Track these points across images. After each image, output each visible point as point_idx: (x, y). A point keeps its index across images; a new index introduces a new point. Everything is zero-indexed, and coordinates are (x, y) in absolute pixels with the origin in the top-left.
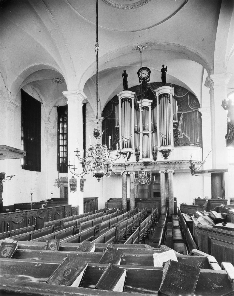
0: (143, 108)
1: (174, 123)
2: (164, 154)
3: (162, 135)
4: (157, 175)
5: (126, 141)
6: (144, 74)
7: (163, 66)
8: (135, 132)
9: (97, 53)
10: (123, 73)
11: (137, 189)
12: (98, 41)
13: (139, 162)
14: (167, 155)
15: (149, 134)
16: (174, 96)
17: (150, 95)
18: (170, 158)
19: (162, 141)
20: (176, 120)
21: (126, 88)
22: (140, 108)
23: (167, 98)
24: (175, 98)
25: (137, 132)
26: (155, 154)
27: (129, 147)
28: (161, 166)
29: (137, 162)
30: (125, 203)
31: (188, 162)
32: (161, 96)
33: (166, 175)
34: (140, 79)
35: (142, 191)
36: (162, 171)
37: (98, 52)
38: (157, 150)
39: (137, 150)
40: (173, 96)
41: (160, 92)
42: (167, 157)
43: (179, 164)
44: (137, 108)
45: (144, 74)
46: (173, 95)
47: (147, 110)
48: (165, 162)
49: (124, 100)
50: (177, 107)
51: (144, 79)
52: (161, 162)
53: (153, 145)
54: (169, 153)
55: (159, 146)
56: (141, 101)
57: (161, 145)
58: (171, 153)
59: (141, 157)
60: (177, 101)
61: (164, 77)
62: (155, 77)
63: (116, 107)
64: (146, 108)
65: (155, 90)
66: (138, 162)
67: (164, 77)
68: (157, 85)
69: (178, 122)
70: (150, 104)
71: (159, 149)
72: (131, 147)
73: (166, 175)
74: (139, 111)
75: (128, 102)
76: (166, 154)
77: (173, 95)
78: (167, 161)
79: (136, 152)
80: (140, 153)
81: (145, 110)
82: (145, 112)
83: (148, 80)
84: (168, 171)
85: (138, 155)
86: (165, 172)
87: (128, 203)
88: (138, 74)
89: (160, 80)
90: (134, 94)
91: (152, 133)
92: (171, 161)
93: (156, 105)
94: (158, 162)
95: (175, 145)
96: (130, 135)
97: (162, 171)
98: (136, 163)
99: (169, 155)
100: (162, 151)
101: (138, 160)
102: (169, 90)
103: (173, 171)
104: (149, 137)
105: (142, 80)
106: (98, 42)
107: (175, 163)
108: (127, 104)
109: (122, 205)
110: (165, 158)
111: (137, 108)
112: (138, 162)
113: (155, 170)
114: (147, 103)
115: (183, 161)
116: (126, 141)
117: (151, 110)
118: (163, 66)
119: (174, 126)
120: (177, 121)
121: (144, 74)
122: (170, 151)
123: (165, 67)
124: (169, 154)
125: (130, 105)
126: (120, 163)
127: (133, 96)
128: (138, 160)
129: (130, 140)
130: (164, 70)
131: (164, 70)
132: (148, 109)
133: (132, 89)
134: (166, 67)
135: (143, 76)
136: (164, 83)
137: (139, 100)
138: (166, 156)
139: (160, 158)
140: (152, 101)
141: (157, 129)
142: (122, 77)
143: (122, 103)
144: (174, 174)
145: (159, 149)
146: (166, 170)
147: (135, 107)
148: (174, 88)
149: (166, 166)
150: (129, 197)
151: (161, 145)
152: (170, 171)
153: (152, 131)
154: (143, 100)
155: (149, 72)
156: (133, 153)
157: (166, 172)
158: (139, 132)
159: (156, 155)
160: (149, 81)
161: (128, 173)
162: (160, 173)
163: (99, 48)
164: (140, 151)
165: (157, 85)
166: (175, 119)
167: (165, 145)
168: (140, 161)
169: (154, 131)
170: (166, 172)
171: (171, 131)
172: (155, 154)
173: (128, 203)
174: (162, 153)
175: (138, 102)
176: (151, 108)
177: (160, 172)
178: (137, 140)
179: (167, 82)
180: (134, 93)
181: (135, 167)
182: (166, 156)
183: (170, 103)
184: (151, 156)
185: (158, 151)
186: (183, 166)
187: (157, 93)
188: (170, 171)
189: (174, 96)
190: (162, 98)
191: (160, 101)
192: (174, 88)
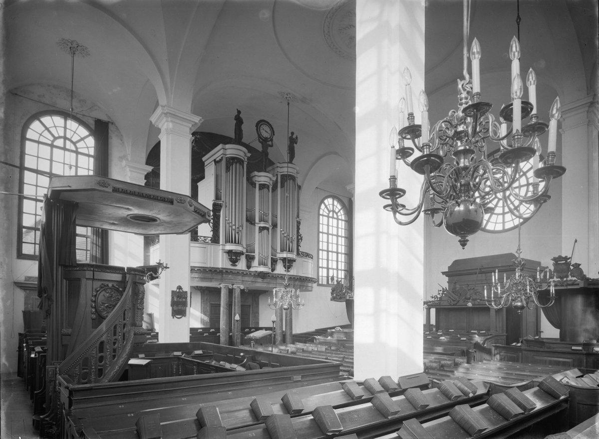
8: (247, 220)
18: (293, 272)
25: (251, 221)
26: (274, 262)
29: (247, 270)
39: (250, 249)
55: (279, 250)
59: (255, 263)
85: (250, 259)
88: (257, 126)
94: (279, 274)
100: (284, 260)
101: (249, 267)
128: (249, 267)
139: (280, 269)
164: (254, 253)
168: (251, 270)
169: (275, 226)
172: (274, 262)
178: (251, 234)
180: (249, 155)
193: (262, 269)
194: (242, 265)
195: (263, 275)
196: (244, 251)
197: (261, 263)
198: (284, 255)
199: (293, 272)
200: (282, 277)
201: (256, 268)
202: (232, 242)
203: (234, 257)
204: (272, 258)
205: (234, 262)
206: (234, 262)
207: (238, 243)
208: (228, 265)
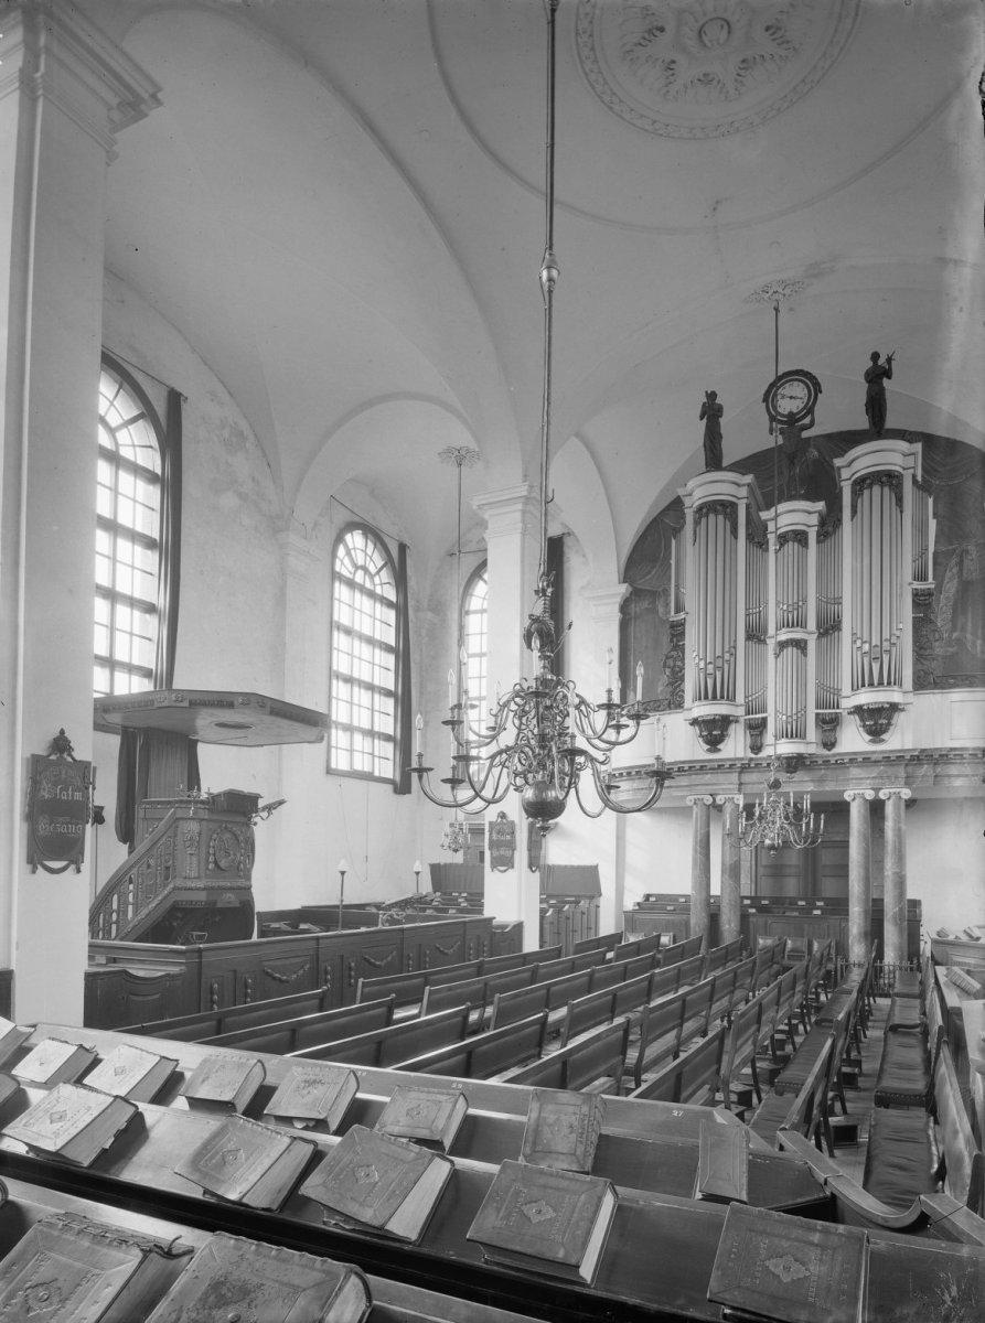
0: (783, 539)
1: (916, 594)
2: (715, 733)
3: (863, 643)
4: (837, 810)
5: (712, 671)
6: (791, 397)
7: (875, 356)
8: (750, 637)
9: (547, 295)
10: (704, 404)
11: (753, 862)
12: (554, 247)
13: (760, 755)
14: (882, 725)
15: (806, 642)
16: (919, 479)
17: (820, 484)
18: (895, 741)
19: (860, 670)
20: (926, 579)
21: (714, 460)
22: (772, 538)
23: (886, 490)
24: (923, 487)
25: (756, 635)
26: (829, 724)
27: (722, 697)
28: (855, 772)
29: (753, 756)
30: (697, 921)
31: (976, 755)
32: (861, 484)
33: (876, 809)
34: (772, 419)
35: (777, 871)
36: (856, 792)
37: (550, 292)
38: (838, 708)
40: (915, 481)
41: (857, 465)
42: (884, 737)
43: (935, 764)
44: (757, 537)
45: (791, 397)
46: (914, 476)
47: (800, 542)
48: (874, 757)
49: (704, 510)
50: (933, 524)
51: (792, 418)
52: (855, 753)
53: (820, 686)
54: (890, 718)
56: (773, 509)
57: (855, 687)
58: (899, 718)
59: (769, 737)
60: (931, 501)
61: (876, 405)
62: (841, 409)
63: (673, 541)
64: (800, 537)
65: (838, 462)
66: (756, 754)
67: (876, 405)
68: (849, 439)
69: (933, 586)
70: (814, 519)
71: (848, 703)
72: (728, 697)
73: (876, 809)
74: (767, 550)
75: (721, 517)
76: (877, 720)
77: (914, 476)
78: (882, 752)
79: (751, 716)
80: (764, 721)
81: (791, 543)
82: (791, 552)
83: (807, 421)
84: (882, 795)
85: (757, 728)
86: (870, 795)
87: (714, 919)
89: (862, 422)
90: (749, 485)
91: (821, 635)
92: (900, 751)
93: (838, 522)
95: (921, 683)
96: (726, 649)
97: (857, 793)
98: (751, 759)
99: (892, 728)
100: (858, 710)
101: (757, 748)
102: (895, 455)
103: (906, 793)
104: (806, 655)
105: (781, 422)
106: (551, 248)
107: (919, 759)
108: (717, 522)
109: (687, 924)
110: (708, 750)
111: (757, 537)
112: (756, 754)
113: (829, 787)
114: (795, 514)
115: (952, 749)
116: (712, 671)
117: (818, 542)
118: (875, 356)
119: (916, 605)
120: (930, 584)
121: (791, 400)
122: (894, 708)
123: (882, 361)
124: (889, 724)
125: (728, 527)
126: (684, 762)
127: (744, 492)
129: (726, 666)
130: (878, 374)
131: (878, 374)
132: (806, 539)
133: (740, 467)
134: (889, 360)
135: (786, 406)
136: (878, 427)
137: (768, 508)
138: (876, 733)
139: (853, 739)
140: (821, 506)
141: (840, 622)
142: (702, 419)
143: (697, 523)
144: (910, 804)
145: (848, 703)
146: (877, 790)
147: (750, 537)
148: (918, 447)
149: (875, 772)
150: (719, 894)
151: (855, 687)
152: (891, 790)
153: (818, 627)
154: (782, 507)
155: (814, 385)
156: (737, 722)
157: (877, 794)
158: (766, 632)
159: (835, 727)
160: (812, 424)
161: (714, 800)
162: (848, 799)
163: (554, 273)
164: (765, 711)
165: (849, 439)
166: (920, 576)
167: (876, 682)
168: (767, 752)
169: (829, 627)
170: (877, 794)
171: (901, 626)
173: (714, 919)
174: (862, 720)
175: (764, 515)
176: (819, 534)
177: (847, 796)
179: (890, 423)
180: (749, 478)
181: (747, 778)
182: (876, 733)
183: (901, 512)
184: (812, 733)
185: (845, 713)
186: (953, 770)
187: (845, 474)
188: (891, 790)
189: (919, 479)
190: (866, 492)
191: (859, 505)
192: (918, 447)
193: (787, 748)
194: (735, 745)
195: (795, 764)
196: (740, 711)
197: (797, 734)
198: (866, 698)
199: (895, 741)
200: (866, 760)
201: (779, 747)
202: (706, 698)
203: (714, 730)
204: (817, 714)
205: (714, 742)
206: (714, 742)
207: (722, 697)
208: (700, 752)
